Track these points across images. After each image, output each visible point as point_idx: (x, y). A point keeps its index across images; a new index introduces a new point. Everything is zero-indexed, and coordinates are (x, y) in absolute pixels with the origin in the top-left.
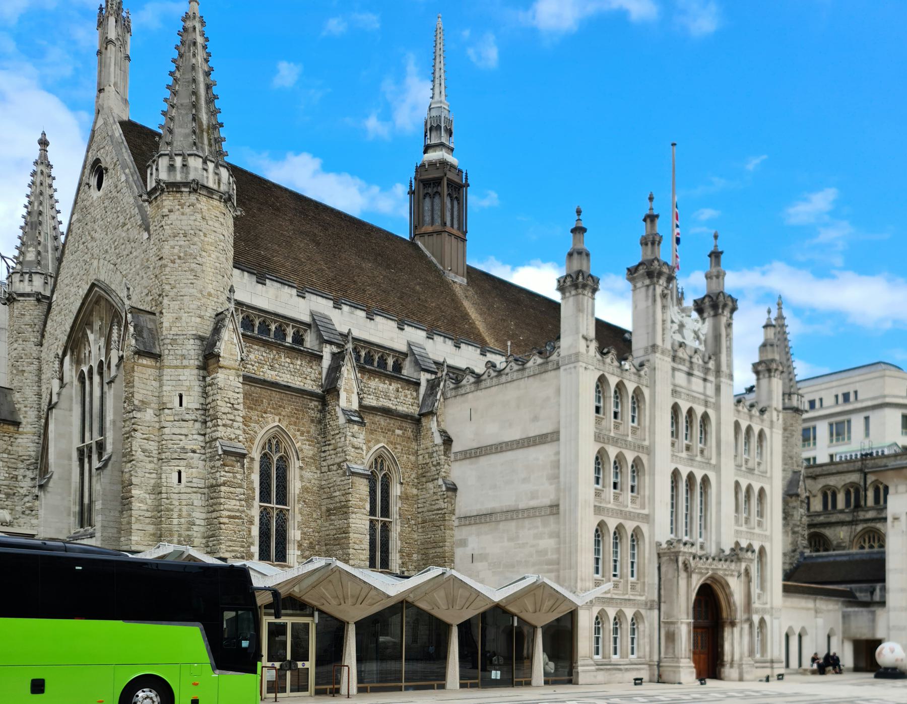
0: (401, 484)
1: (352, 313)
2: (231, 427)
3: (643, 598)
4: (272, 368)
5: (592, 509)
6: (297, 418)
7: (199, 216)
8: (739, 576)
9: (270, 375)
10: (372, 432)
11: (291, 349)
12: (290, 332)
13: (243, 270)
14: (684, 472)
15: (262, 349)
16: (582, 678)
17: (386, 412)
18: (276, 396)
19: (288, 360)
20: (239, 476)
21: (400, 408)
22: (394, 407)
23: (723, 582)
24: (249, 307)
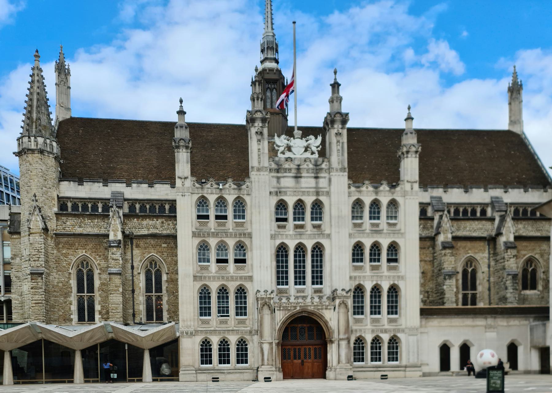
0: (167, 274)
1: (139, 187)
2: (38, 261)
3: (249, 328)
4: (80, 227)
5: (192, 278)
6: (96, 249)
7: (28, 164)
8: (335, 308)
9: (79, 230)
10: (145, 248)
11: (91, 215)
12: (100, 205)
13: (70, 181)
14: (292, 245)
15: (74, 218)
16: (181, 377)
17: (154, 236)
18: (83, 240)
19: (89, 221)
20: (39, 284)
21: (165, 232)
22: (160, 232)
23: (318, 314)
24: (73, 198)
